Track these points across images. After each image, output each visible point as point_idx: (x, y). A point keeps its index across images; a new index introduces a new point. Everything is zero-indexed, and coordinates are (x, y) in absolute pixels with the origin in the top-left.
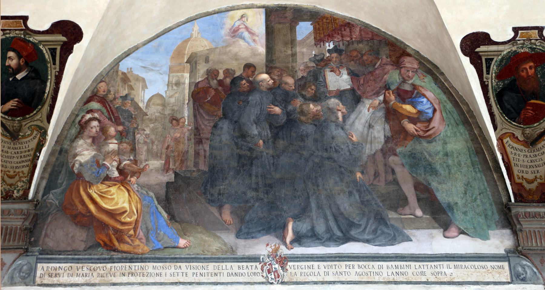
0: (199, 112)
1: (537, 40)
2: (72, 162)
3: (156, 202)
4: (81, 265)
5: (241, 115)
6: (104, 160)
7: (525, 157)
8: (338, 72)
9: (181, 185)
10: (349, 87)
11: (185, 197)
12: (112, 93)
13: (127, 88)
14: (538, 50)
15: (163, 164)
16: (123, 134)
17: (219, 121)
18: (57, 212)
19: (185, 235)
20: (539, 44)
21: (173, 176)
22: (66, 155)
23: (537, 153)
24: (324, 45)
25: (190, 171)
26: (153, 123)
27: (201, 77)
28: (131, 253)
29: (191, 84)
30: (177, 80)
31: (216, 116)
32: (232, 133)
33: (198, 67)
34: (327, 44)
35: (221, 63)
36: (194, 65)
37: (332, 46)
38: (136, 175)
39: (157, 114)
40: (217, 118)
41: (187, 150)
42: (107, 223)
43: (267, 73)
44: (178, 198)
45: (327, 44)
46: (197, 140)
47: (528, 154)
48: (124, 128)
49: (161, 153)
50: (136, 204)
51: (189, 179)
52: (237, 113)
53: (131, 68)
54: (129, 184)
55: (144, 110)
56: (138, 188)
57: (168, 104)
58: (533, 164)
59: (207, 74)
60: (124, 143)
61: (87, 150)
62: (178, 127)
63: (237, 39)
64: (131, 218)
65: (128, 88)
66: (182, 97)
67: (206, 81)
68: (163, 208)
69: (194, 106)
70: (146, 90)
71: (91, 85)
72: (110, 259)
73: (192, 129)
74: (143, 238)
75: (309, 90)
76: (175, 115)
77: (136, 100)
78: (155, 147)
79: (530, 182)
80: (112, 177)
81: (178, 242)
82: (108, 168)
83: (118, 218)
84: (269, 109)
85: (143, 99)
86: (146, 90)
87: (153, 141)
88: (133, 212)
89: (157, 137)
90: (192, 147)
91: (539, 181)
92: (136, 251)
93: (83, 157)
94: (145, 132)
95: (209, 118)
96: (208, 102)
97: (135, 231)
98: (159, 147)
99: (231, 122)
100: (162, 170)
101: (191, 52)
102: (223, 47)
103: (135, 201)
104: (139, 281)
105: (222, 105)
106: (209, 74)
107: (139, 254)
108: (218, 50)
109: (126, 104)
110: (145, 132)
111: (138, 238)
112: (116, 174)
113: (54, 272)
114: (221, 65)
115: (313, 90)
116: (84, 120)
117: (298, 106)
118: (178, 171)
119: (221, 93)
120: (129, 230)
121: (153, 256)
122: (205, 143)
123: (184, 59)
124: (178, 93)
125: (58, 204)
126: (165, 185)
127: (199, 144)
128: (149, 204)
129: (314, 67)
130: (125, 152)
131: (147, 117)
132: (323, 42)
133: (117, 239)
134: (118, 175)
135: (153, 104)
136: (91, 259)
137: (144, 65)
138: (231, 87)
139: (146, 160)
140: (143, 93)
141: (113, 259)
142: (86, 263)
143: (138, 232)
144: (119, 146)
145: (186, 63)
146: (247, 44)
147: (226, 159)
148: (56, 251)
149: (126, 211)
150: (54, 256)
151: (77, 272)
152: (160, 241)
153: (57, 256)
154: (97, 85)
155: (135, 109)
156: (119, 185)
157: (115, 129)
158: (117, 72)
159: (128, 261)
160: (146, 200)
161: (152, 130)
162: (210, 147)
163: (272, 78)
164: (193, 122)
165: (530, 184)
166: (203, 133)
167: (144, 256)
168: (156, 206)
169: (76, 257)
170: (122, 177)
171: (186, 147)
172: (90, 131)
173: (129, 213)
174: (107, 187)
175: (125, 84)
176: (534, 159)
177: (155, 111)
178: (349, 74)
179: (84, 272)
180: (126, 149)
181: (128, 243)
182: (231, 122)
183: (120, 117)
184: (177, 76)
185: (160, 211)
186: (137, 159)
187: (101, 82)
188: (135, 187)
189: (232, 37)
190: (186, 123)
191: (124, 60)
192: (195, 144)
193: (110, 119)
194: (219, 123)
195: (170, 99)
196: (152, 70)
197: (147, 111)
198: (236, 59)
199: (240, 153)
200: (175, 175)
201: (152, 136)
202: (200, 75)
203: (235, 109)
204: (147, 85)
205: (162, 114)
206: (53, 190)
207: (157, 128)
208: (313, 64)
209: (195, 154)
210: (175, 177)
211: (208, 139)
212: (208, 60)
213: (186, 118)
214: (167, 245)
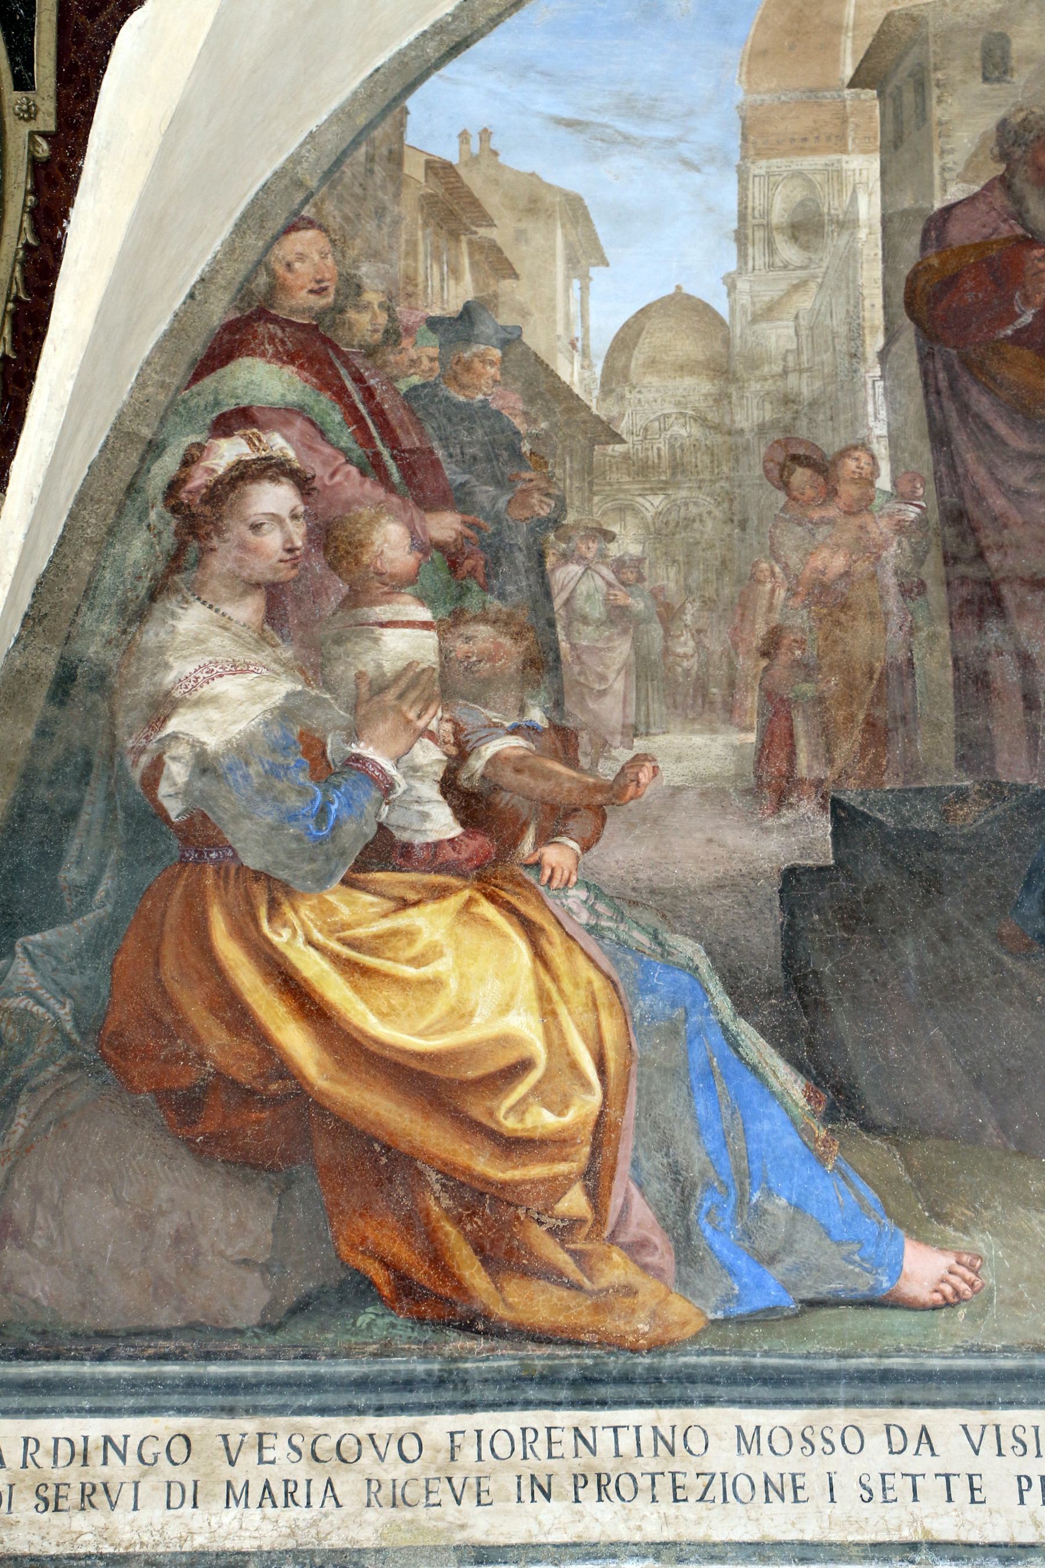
0: (965, 409)
2: (142, 751)
3: (724, 1003)
4: (250, 1425)
6: (355, 734)
9: (880, 890)
11: (920, 968)
12: (373, 297)
13: (466, 261)
15: (750, 752)
16: (469, 564)
18: (70, 1078)
19: (941, 1218)
21: (824, 827)
22: (104, 706)
25: (938, 793)
26: (662, 488)
27: (962, 178)
28: (579, 1344)
29: (897, 225)
30: (802, 204)
33: (937, 112)
36: (909, 97)
38: (572, 824)
39: (681, 431)
41: (901, 656)
42: (404, 1147)
44: (866, 976)
46: (964, 592)
48: (471, 526)
49: (732, 684)
50: (588, 1018)
51: (930, 848)
53: (485, 134)
54: (532, 887)
55: (593, 405)
56: (592, 910)
57: (754, 363)
59: (1004, 156)
60: (475, 619)
61: (238, 669)
62: (832, 512)
64: (561, 1107)
65: (473, 265)
66: (840, 313)
67: (999, 199)
68: (774, 1042)
69: (925, 373)
70: (594, 272)
71: (230, 249)
72: (441, 1382)
73: (922, 522)
74: (657, 1238)
76: (803, 431)
77: (535, 339)
78: (685, 645)
80: (418, 840)
81: (896, 1269)
82: (387, 788)
83: (476, 1111)
85: (577, 332)
86: (594, 272)
87: (668, 606)
88: (574, 1066)
89: (696, 576)
90: (933, 637)
92: (614, 1324)
93: (213, 713)
94: (614, 550)
96: (1017, 338)
97: (597, 1196)
98: (715, 644)
100: (747, 792)
101: (880, 14)
103: (579, 998)
104: (654, 1531)
106: (1018, 153)
107: (635, 1350)
109: (468, 368)
110: (614, 550)
111: (622, 1239)
113: (74, 1475)
116: (199, 479)
118: (851, 796)
120: (557, 1188)
121: (734, 1360)
122: (1022, 608)
123: (836, 61)
124: (813, 286)
125: (69, 1026)
126: (771, 888)
127: (981, 615)
128: (678, 1013)
130: (487, 682)
131: (619, 448)
133: (479, 1249)
134: (457, 831)
135: (652, 364)
136: (316, 1384)
137: (567, 113)
139: (633, 731)
140: (575, 293)
141: (464, 1382)
142: (280, 1410)
143: (615, 1203)
144: (442, 638)
145: (852, 84)
148: (75, 1335)
149: (525, 1065)
150: (66, 1369)
151: (226, 1471)
152: (772, 1260)
153: (88, 1369)
154: (268, 249)
155: (530, 401)
156: (466, 893)
157: (413, 533)
158: (396, 158)
159: (564, 1394)
160: (653, 990)
161: (658, 532)
164: (927, 473)
166: (1000, 547)
167: (668, 1361)
168: (725, 1029)
169: (215, 1369)
170: (480, 843)
171: (895, 636)
172: (243, 546)
173: (547, 1077)
174: (390, 905)
175: (454, 235)
177: (669, 409)
179: (276, 1476)
180: (491, 658)
181: (553, 1275)
183: (440, 453)
184: (799, 174)
185: (753, 1057)
186: (570, 724)
187: (290, 228)
188: (571, 903)
190: (884, 482)
191: (433, 78)
192: (955, 617)
193: (373, 468)
195: (762, 327)
196: (627, 138)
197: (615, 411)
200: (836, 820)
201: (661, 572)
202: (957, 160)
204: (603, 240)
205: (716, 428)
206: (33, 931)
207: (688, 523)
209: (958, 686)
210: (834, 834)
212: (1005, 56)
213: (881, 450)
214: (825, 1289)
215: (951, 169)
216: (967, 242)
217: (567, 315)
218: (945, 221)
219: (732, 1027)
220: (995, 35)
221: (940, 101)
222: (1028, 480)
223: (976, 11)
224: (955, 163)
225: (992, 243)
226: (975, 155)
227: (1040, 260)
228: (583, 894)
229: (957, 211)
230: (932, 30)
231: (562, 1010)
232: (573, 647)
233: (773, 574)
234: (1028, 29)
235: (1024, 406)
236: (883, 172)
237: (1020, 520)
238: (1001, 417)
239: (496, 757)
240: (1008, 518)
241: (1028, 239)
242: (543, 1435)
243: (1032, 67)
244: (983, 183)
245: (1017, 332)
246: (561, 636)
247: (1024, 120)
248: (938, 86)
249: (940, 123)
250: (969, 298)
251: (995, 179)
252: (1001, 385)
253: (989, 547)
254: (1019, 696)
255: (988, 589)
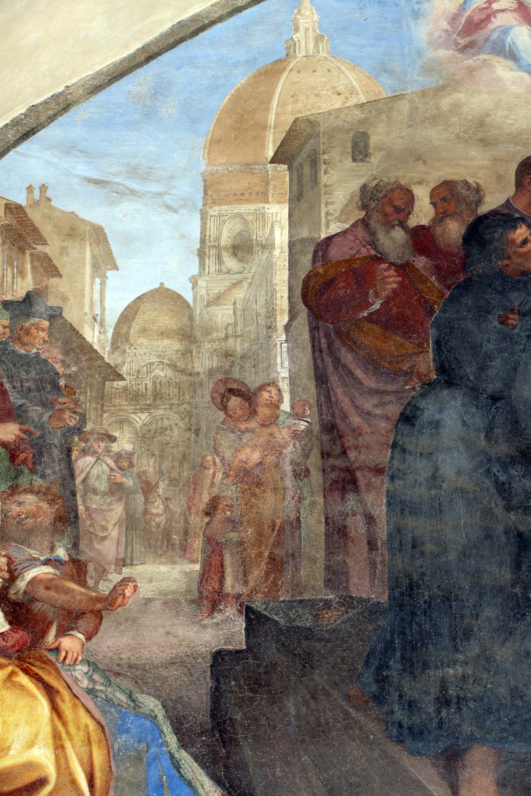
0: (337, 362)
3: (172, 740)
5: (515, 369)
9: (274, 665)
11: (298, 717)
13: (29, 266)
15: (196, 577)
16: (22, 456)
17: (423, 396)
21: (240, 624)
25: (312, 603)
26: (147, 408)
27: (338, 219)
29: (298, 248)
30: (240, 233)
31: (409, 374)
32: (482, 442)
33: (324, 179)
35: (419, 158)
36: (307, 170)
38: (80, 622)
39: (160, 373)
40: (416, 383)
41: (293, 516)
44: (263, 722)
46: (333, 476)
48: (25, 432)
49: (186, 533)
50: (84, 750)
51: (307, 638)
52: (497, 363)
53: (43, 188)
54: (52, 664)
55: (106, 356)
56: (91, 679)
57: (207, 331)
59: (364, 207)
60: (25, 491)
62: (253, 424)
63: (482, 57)
65: (33, 268)
66: (262, 301)
67: (361, 232)
68: (203, 765)
69: (313, 339)
70: (109, 273)
73: (309, 432)
76: (236, 375)
85: (98, 311)
86: (109, 273)
87: (148, 483)
88: (74, 782)
89: (167, 464)
90: (313, 504)
94: (115, 447)
95: (382, 386)
96: (370, 319)
98: (176, 508)
99: (477, 398)
100: (193, 602)
101: (291, 119)
102: (423, 94)
103: (79, 736)
105: (432, 333)
106: (373, 205)
108: (405, 106)
109: (28, 333)
110: (115, 447)
114: (421, 167)
118: (258, 605)
119: (424, 280)
122: (369, 485)
123: (263, 146)
124: (245, 284)
126: (206, 664)
127: (343, 491)
128: (143, 746)
130: (31, 531)
131: (121, 383)
135: (144, 331)
137: (95, 175)
138: (467, 255)
139: (122, 563)
140: (97, 287)
145: (272, 161)
147: (464, 554)
149: (42, 782)
155: (66, 353)
156: (10, 668)
160: (127, 731)
161: (144, 436)
162: (389, 504)
164: (313, 401)
166: (356, 448)
168: (172, 757)
170: (20, 635)
171: (290, 503)
175: (22, 250)
177: (154, 359)
180: (34, 516)
182: (477, 398)
183: (7, 386)
184: (239, 215)
185: (189, 775)
186: (82, 558)
188: (77, 674)
189: (464, 49)
190: (286, 406)
191: (11, 153)
192: (327, 491)
194: (422, 404)
195: (213, 309)
196: (132, 191)
197: (119, 361)
198: (481, 140)
199: (522, 528)
200: (248, 620)
201: (145, 462)
202: (336, 208)
203: (491, 346)
204: (116, 253)
205: (183, 371)
207: (163, 430)
209: (327, 535)
210: (246, 629)
211: (379, 471)
212: (366, 146)
213: (285, 386)
215: (331, 214)
216: (341, 259)
217: (92, 299)
218: (328, 245)
219: (177, 755)
220: (360, 133)
221: (326, 173)
222: (376, 406)
223: (349, 119)
224: (334, 210)
225: (356, 260)
226: (347, 206)
227: (385, 270)
228: (85, 669)
229: (335, 240)
230: (322, 129)
231: (68, 745)
232: (87, 509)
233: (215, 463)
234: (380, 130)
235: (373, 360)
236: (290, 215)
237: (369, 431)
238: (359, 367)
239: (34, 579)
240: (362, 430)
241: (378, 258)
243: (382, 153)
244: (351, 223)
245: (370, 314)
247: (377, 185)
248: (325, 163)
249: (326, 186)
250: (342, 293)
251: (358, 220)
252: (359, 347)
253: (349, 448)
254: (365, 542)
255: (348, 474)
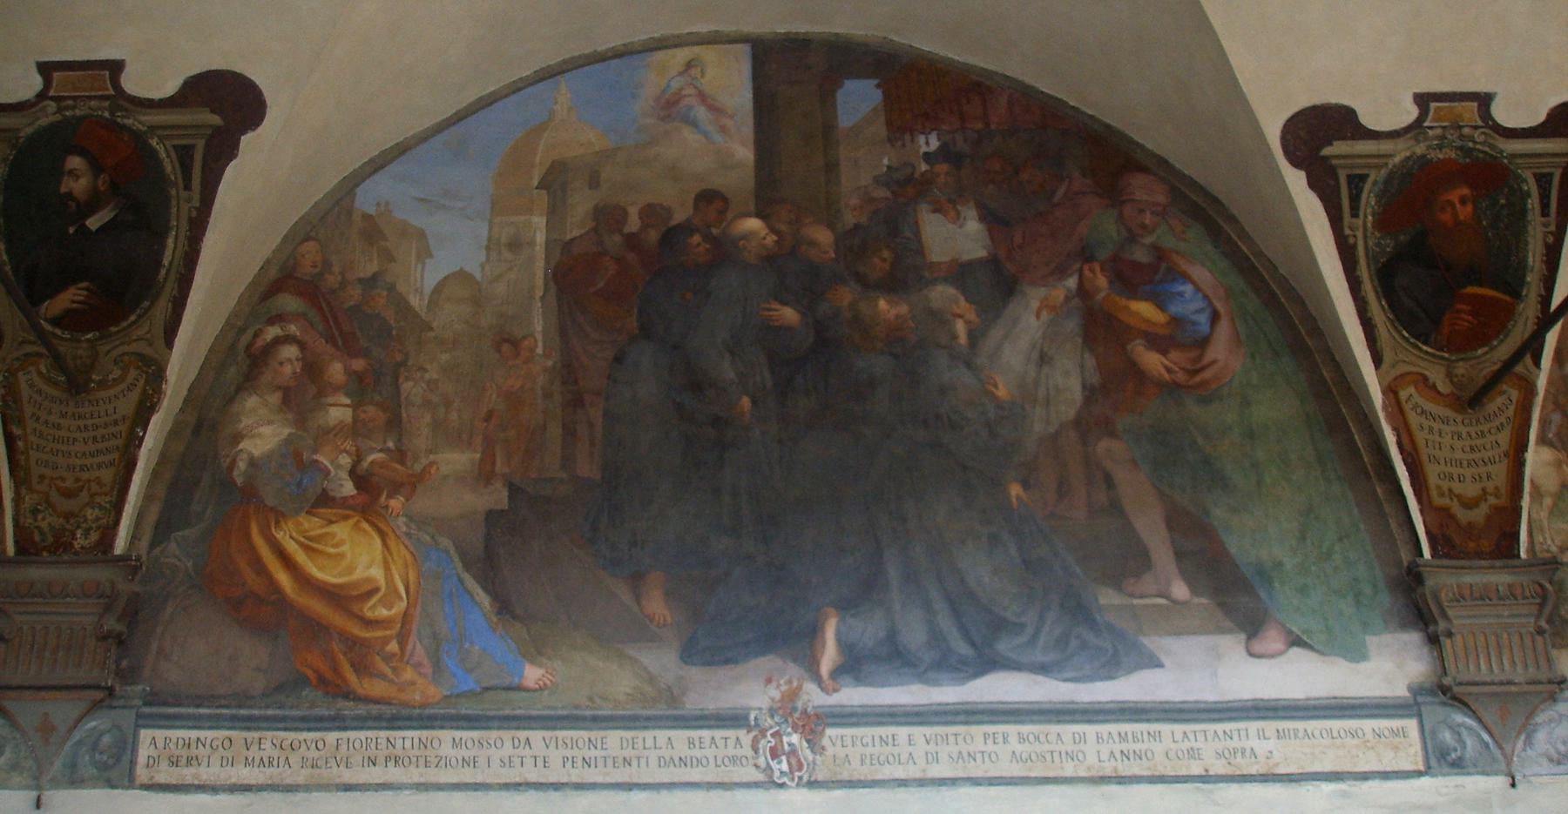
1: (1476, 128)
2: (228, 456)
3: (459, 565)
4: (256, 735)
6: (315, 451)
7: (1456, 437)
8: (952, 213)
10: (981, 253)
12: (336, 269)
13: (375, 255)
14: (1481, 155)
18: (190, 592)
19: (540, 653)
20: (1482, 138)
23: (1485, 428)
24: (912, 141)
28: (390, 704)
34: (922, 139)
37: (934, 144)
43: (759, 215)
45: (922, 139)
47: (1464, 430)
48: (369, 364)
56: (408, 526)
58: (1476, 456)
61: (270, 422)
62: (517, 362)
64: (389, 608)
70: (427, 261)
71: (279, 249)
72: (333, 719)
74: (426, 662)
75: (876, 260)
77: (401, 287)
78: (454, 416)
79: (1469, 504)
80: (338, 495)
81: (521, 676)
82: (328, 473)
83: (356, 609)
84: (767, 313)
86: (427, 261)
88: (396, 591)
91: (1492, 500)
92: (404, 696)
93: (258, 442)
94: (427, 376)
97: (402, 645)
104: (416, 779)
110: (427, 376)
111: (411, 662)
112: (348, 488)
113: (184, 753)
115: (884, 260)
116: (260, 343)
117: (845, 303)
120: (386, 640)
121: (453, 711)
125: (190, 570)
129: (887, 199)
132: (912, 135)
133: (352, 665)
134: (355, 492)
136: (283, 719)
140: (419, 270)
141: (344, 719)
142: (268, 729)
143: (409, 647)
144: (354, 411)
145: (537, 188)
146: (703, 139)
148: (187, 697)
150: (183, 710)
151: (245, 752)
152: (472, 670)
153: (191, 710)
154: (295, 248)
156: (356, 518)
157: (345, 367)
158: (350, 213)
159: (384, 724)
163: (772, 230)
165: (1470, 508)
167: (428, 711)
169: (243, 712)
173: (385, 595)
176: (1479, 442)
178: (982, 219)
179: (265, 755)
181: (383, 676)
183: (359, 334)
186: (403, 448)
187: (303, 242)
189: (663, 119)
190: (539, 351)
193: (330, 339)
206: (178, 531)
208: (882, 193)
210: (509, 496)
213: (539, 337)
214: (492, 683)
217: (416, 277)
219: (462, 576)
228: (405, 519)
231: (393, 568)
232: (408, 416)
233: (491, 387)
236: (547, 222)
239: (372, 462)
242: (374, 740)
246: (403, 411)
